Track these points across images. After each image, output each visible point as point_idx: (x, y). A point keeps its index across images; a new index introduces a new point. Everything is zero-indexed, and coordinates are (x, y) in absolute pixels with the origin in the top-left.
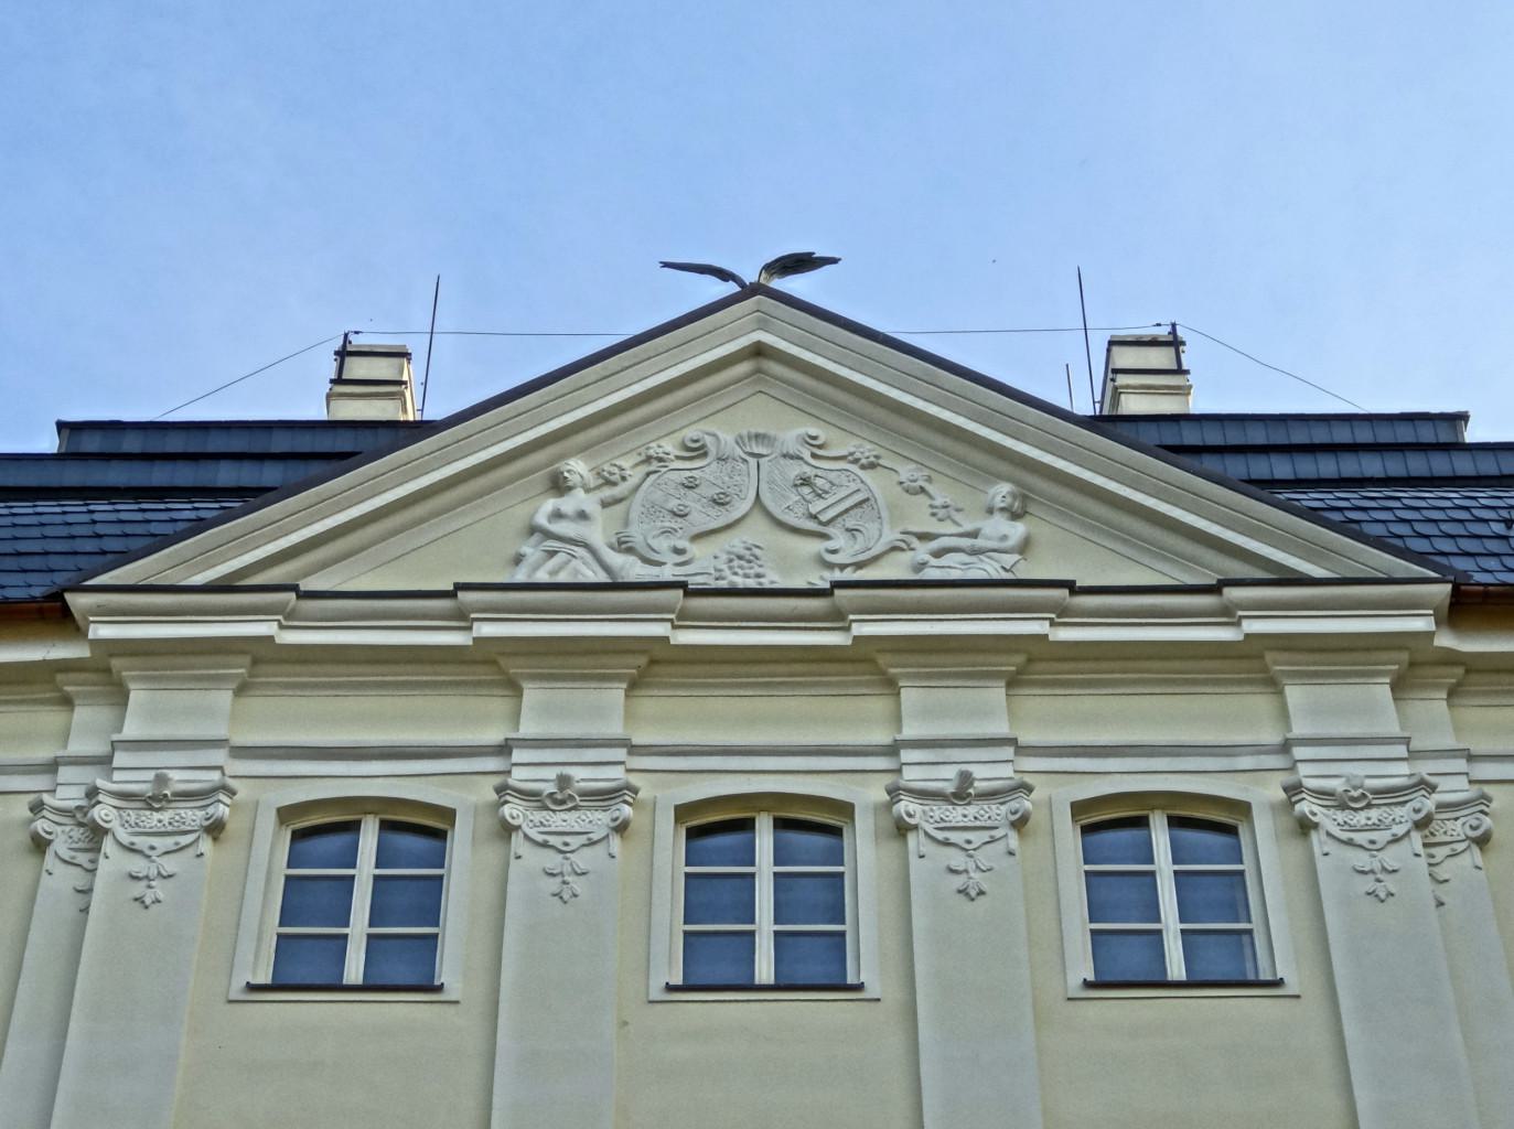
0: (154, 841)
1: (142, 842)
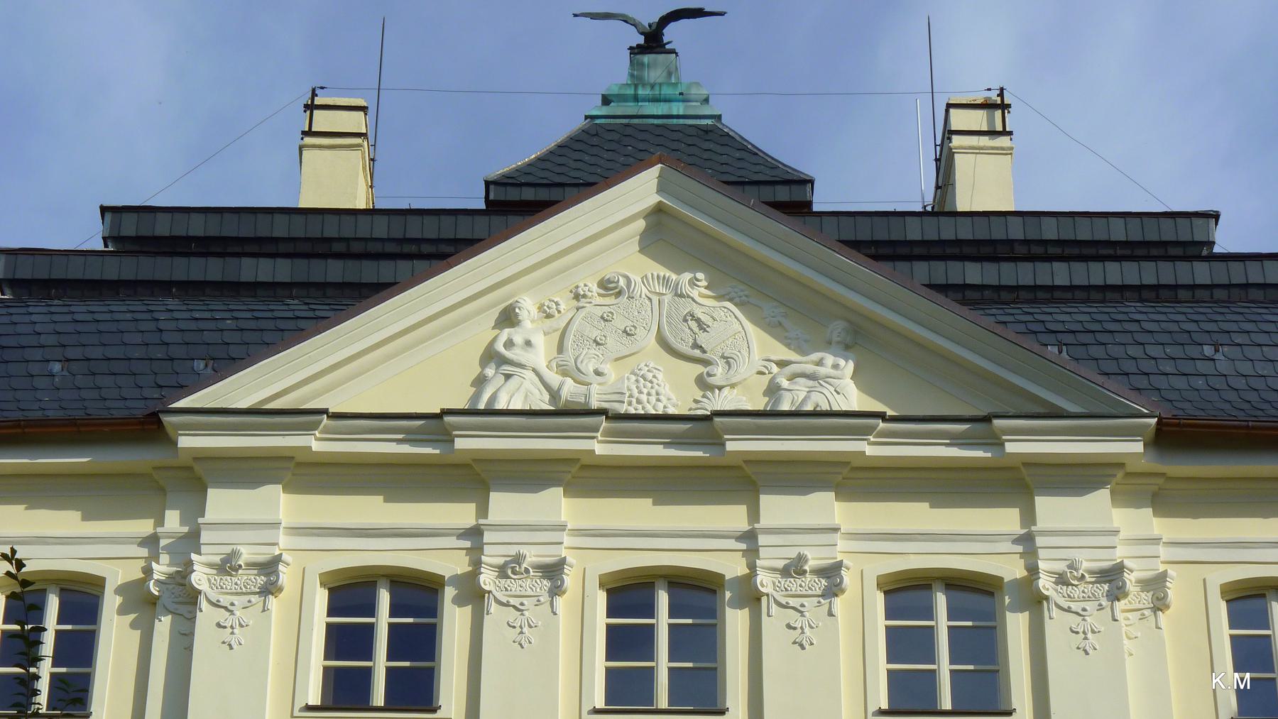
0: (235, 599)
1: (225, 600)
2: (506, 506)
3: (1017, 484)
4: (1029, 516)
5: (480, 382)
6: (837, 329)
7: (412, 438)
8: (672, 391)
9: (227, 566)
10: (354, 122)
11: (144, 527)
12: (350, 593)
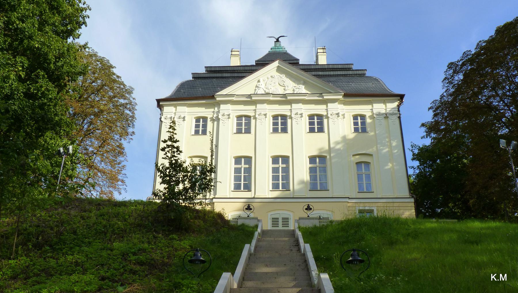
2: (259, 106)
3: (326, 102)
4: (327, 106)
5: (255, 90)
6: (302, 82)
7: (247, 98)
8: (281, 91)
9: (223, 115)
10: (237, 53)
11: (213, 110)
12: (239, 117)
